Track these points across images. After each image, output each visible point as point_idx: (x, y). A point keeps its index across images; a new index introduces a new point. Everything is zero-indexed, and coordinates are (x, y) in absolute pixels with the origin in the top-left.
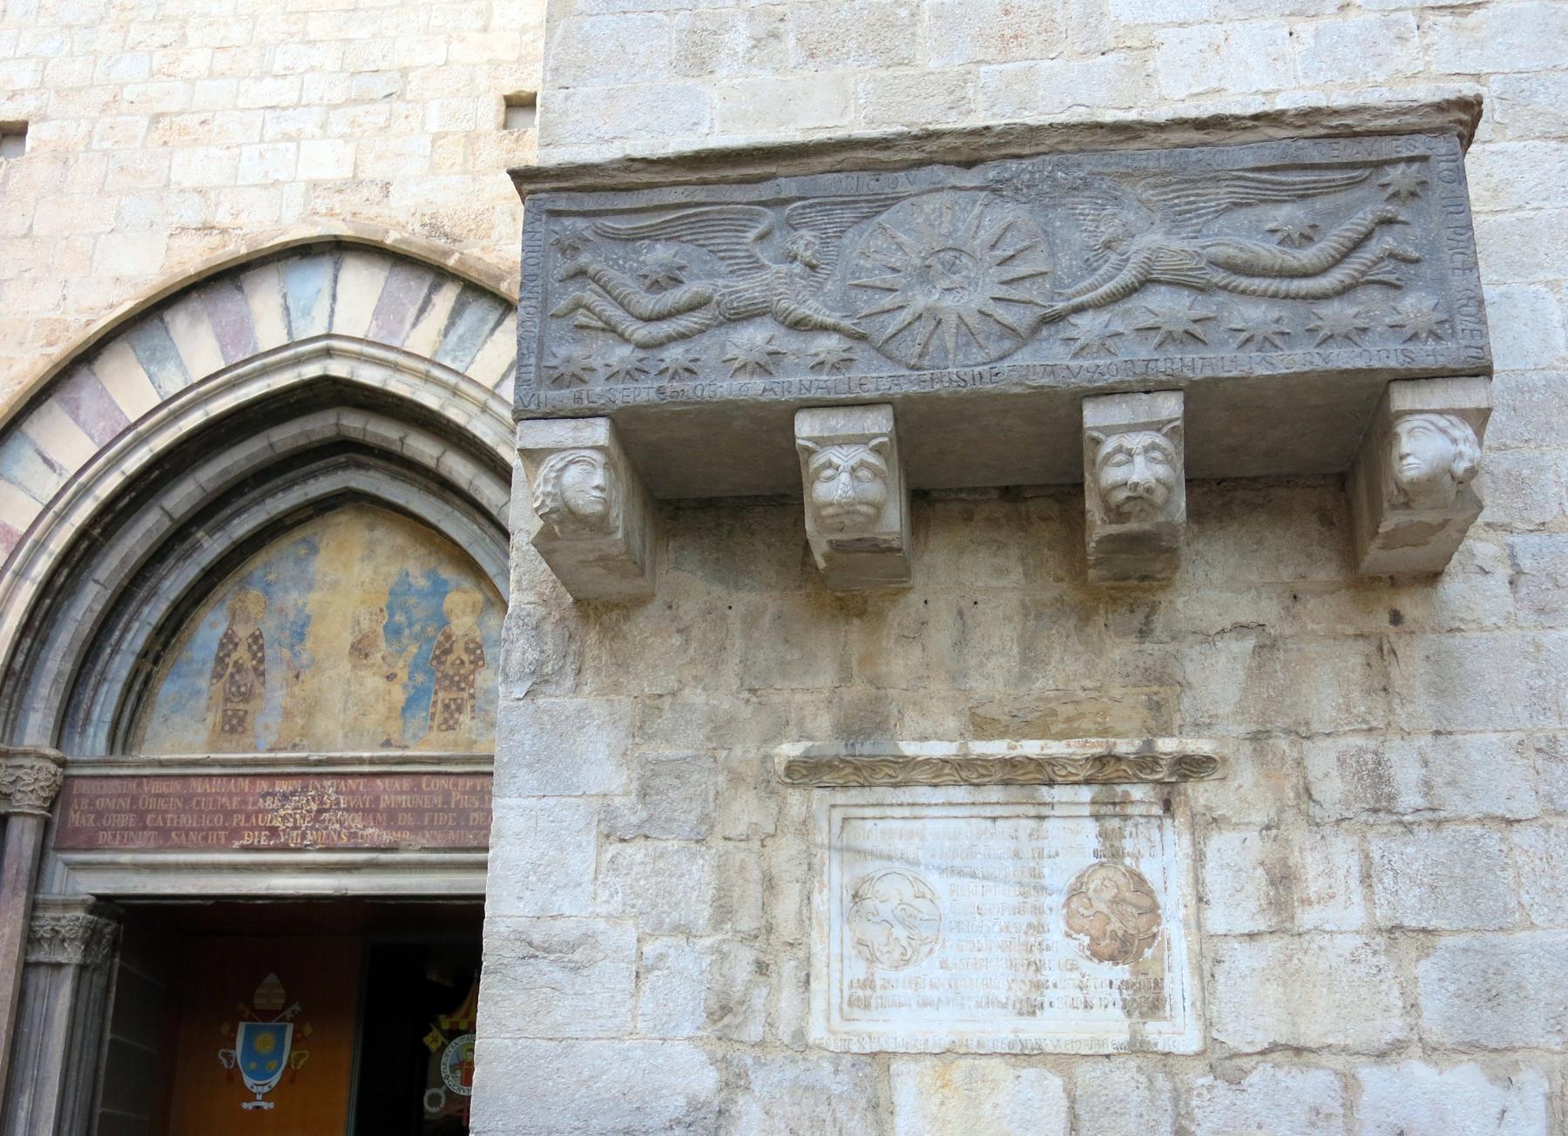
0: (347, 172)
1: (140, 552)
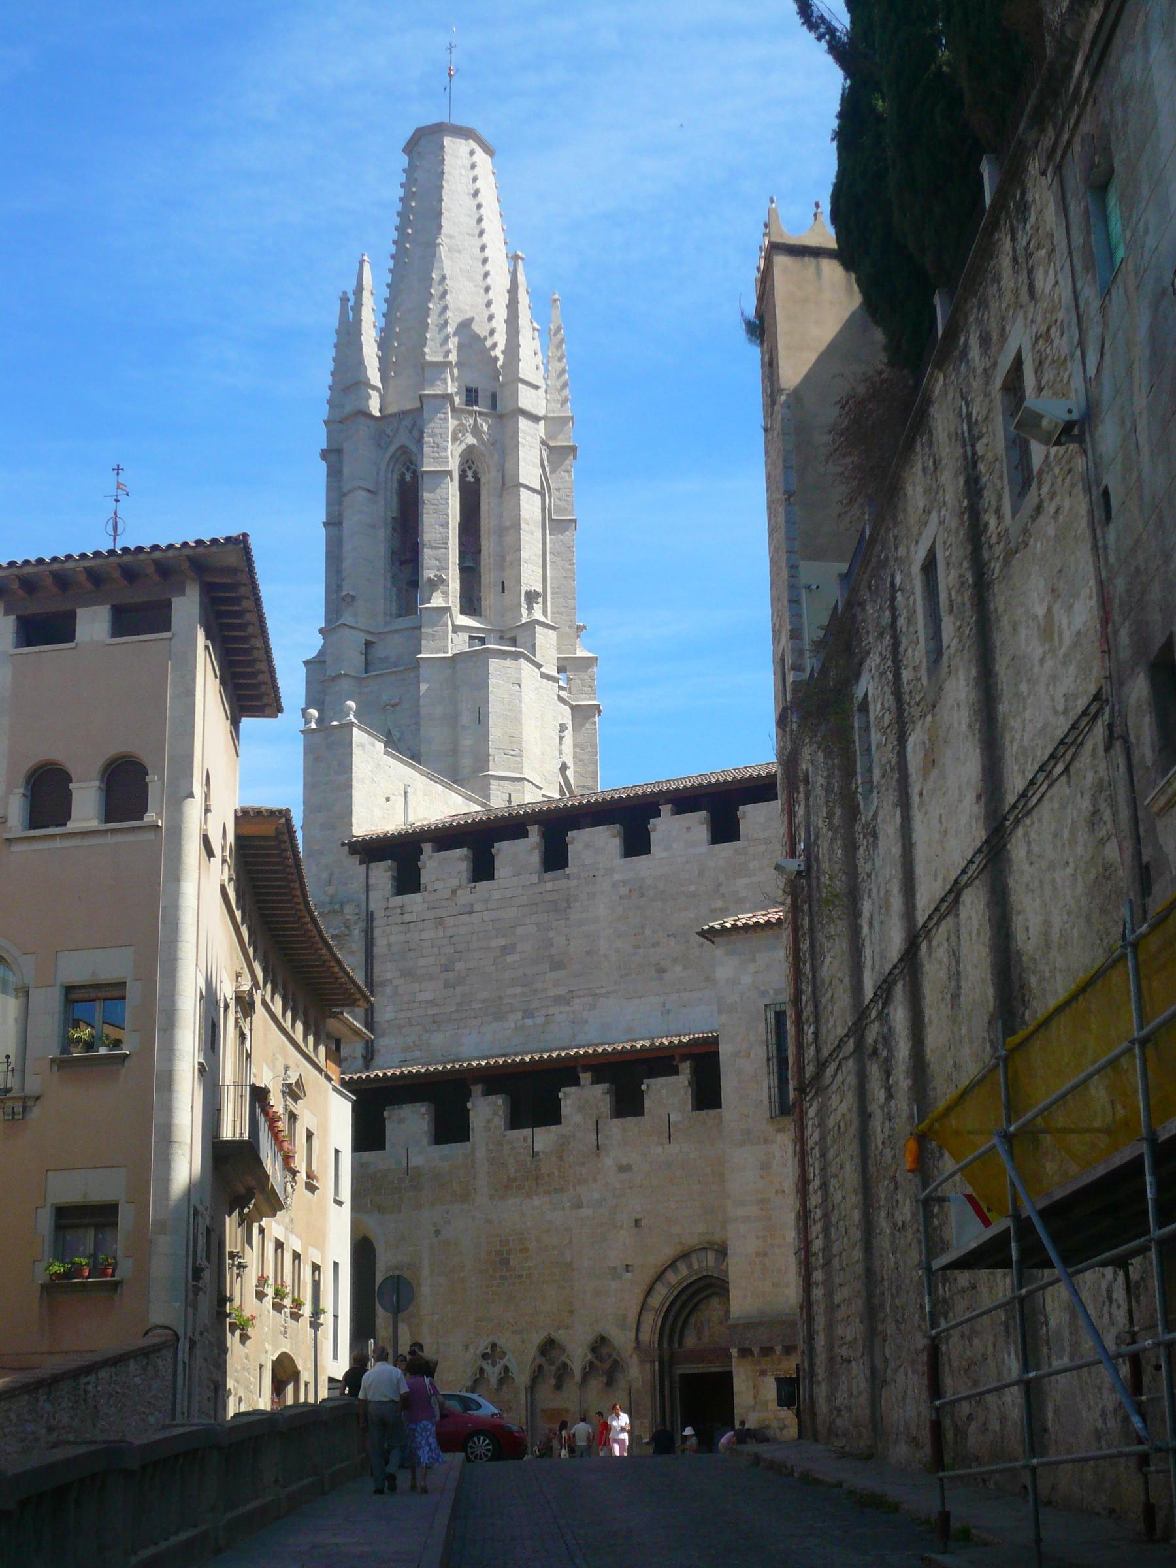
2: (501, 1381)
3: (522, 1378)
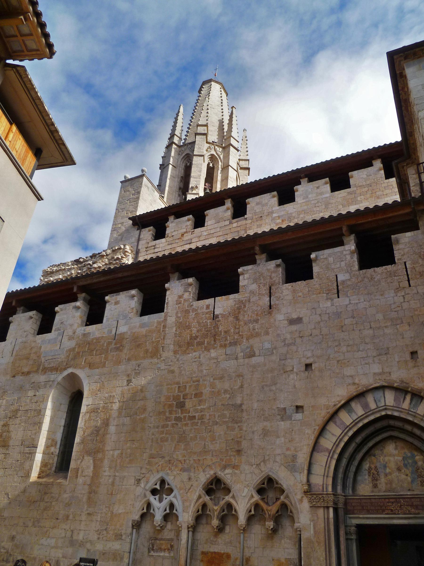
0: (381, 370)
1: (352, 452)
2: (166, 517)
3: (186, 517)
